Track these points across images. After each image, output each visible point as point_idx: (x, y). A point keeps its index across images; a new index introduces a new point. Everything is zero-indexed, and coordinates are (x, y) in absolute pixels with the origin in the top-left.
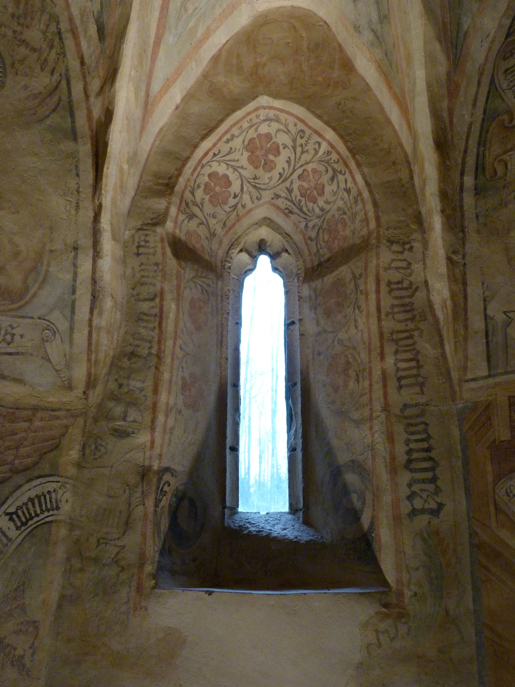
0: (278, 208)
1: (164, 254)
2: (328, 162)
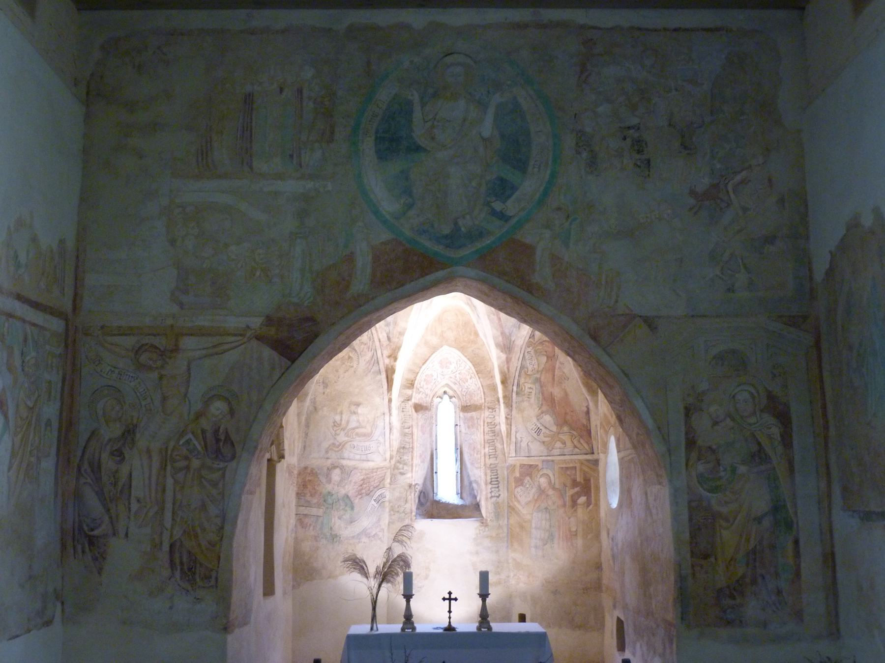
0: (451, 381)
1: (412, 411)
2: (469, 372)
